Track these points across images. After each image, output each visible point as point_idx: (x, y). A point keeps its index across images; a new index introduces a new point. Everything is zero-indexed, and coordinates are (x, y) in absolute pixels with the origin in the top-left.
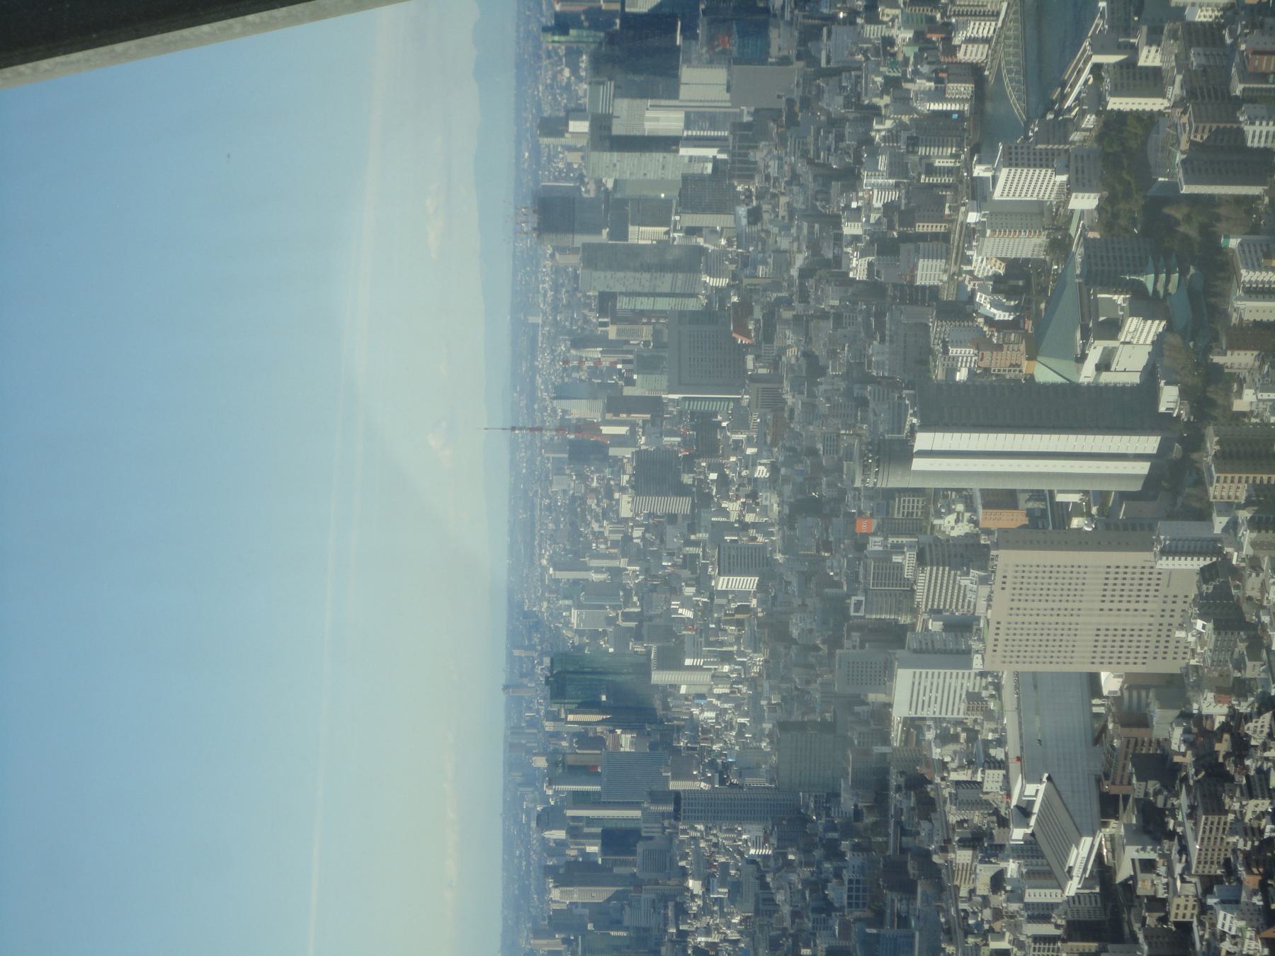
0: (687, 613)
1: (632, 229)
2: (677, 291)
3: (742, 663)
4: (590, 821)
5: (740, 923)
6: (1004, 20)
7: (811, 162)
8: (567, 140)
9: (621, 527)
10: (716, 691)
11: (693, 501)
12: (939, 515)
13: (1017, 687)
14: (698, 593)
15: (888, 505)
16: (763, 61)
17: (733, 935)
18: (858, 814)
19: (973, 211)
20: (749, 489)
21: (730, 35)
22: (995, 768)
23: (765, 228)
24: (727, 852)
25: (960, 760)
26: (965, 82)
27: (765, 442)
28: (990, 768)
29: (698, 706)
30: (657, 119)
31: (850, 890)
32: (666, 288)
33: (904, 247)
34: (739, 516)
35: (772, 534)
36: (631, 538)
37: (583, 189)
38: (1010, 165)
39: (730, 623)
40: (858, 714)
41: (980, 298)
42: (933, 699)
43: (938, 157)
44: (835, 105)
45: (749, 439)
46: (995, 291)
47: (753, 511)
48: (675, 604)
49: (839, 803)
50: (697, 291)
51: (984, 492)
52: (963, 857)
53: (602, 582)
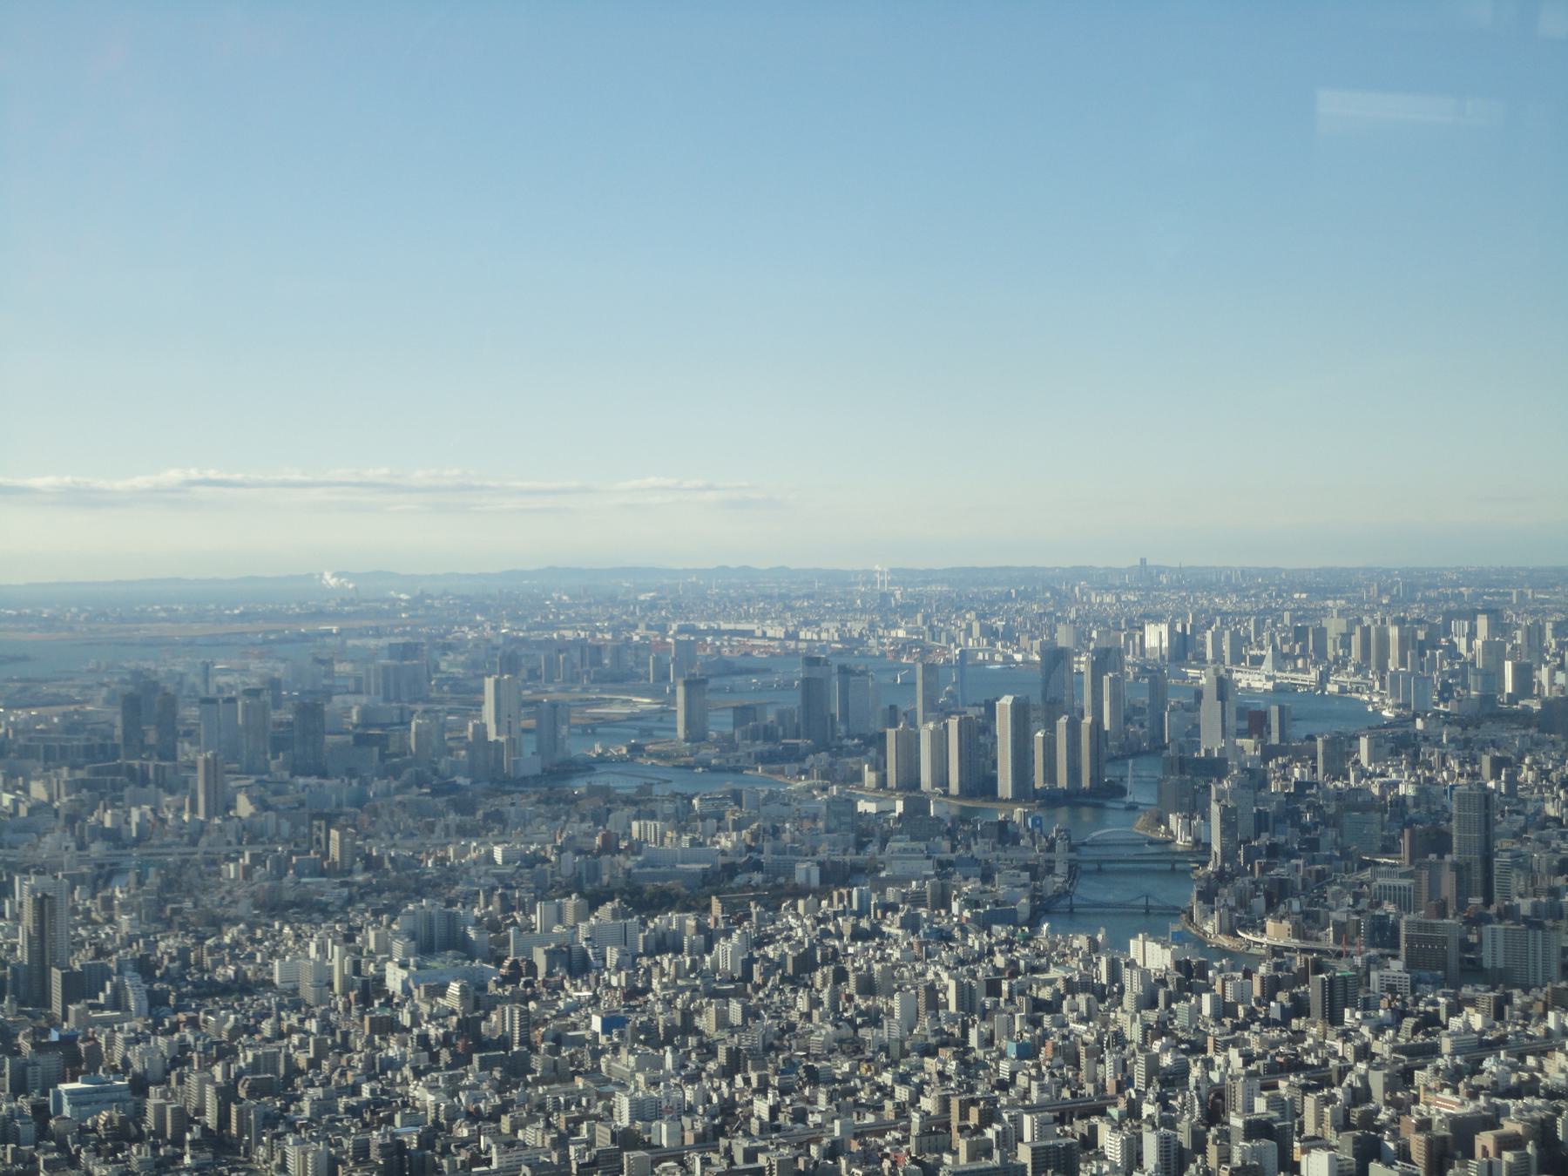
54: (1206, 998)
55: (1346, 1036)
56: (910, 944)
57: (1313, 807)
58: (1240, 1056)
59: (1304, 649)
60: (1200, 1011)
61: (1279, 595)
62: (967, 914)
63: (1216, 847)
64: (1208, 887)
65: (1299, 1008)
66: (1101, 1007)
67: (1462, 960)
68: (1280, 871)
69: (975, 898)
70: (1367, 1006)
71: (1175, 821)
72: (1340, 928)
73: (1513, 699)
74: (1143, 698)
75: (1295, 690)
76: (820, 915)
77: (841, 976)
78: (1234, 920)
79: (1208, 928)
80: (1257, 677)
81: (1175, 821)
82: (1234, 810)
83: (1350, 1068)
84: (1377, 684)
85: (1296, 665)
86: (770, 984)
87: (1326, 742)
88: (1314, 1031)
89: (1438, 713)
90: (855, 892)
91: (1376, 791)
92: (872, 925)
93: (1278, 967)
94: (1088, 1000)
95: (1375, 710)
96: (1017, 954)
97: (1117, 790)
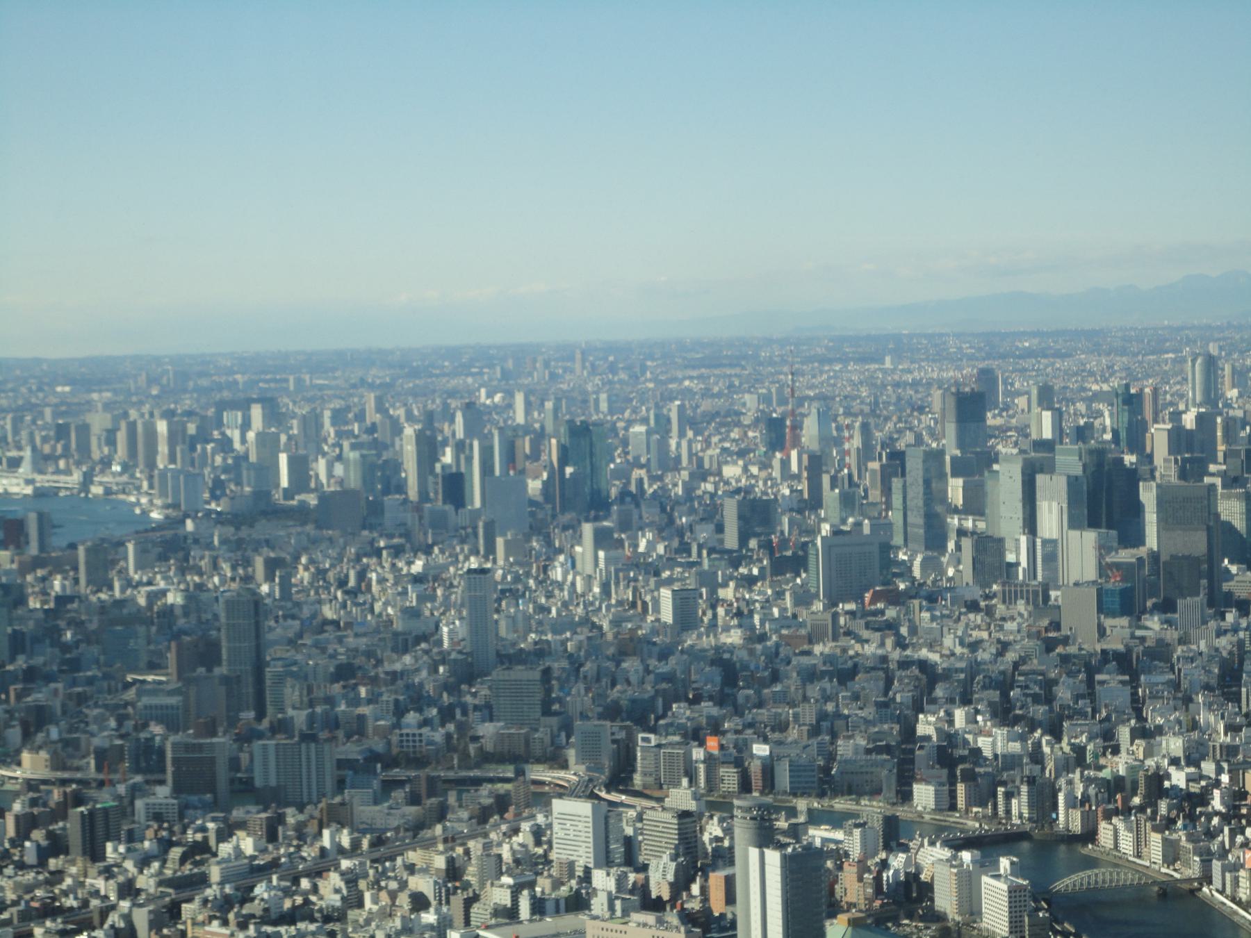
0: (642, 549)
1: (959, 482)
2: (909, 529)
3: (600, 608)
4: (469, 459)
5: (388, 615)
6: (1134, 863)
7: (1016, 665)
8: (1036, 410)
9: (715, 466)
10: (578, 579)
11: (735, 551)
12: (721, 820)
13: (576, 932)
14: (660, 557)
15: (730, 763)
16: (1100, 610)
17: (378, 607)
18: (475, 739)
19: (972, 856)
20: (746, 612)
21: (1121, 581)
22: (512, 897)
23: (962, 617)
24: (446, 598)
25: (520, 852)
26: (1082, 826)
27: (782, 627)
28: (512, 892)
29: (566, 560)
30: (1050, 511)
31: (414, 735)
32: (910, 520)
33: (945, 772)
34: (723, 600)
35: (708, 636)
36: (705, 480)
37: (996, 412)
38: (1010, 892)
39: (635, 590)
40: (559, 736)
41: (902, 857)
42: (568, 832)
43: (1019, 802)
44: (1063, 693)
45: (785, 609)
46: (907, 874)
47: (727, 614)
48: (649, 535)
49: (483, 721)
50: (909, 545)
51: (734, 875)
52: (440, 862)
53: (668, 446)
55: (108, 873)
57: (77, 624)
59: (66, 448)
61: (40, 389)
65: (57, 846)
67: (232, 781)
68: (39, 696)
70: (131, 838)
72: (101, 755)
73: (288, 494)
75: (56, 494)
80: (15, 481)
83: (113, 907)
84: (145, 485)
87: (88, 551)
88: (73, 870)
89: (209, 512)
91: (142, 601)
93: (34, 803)
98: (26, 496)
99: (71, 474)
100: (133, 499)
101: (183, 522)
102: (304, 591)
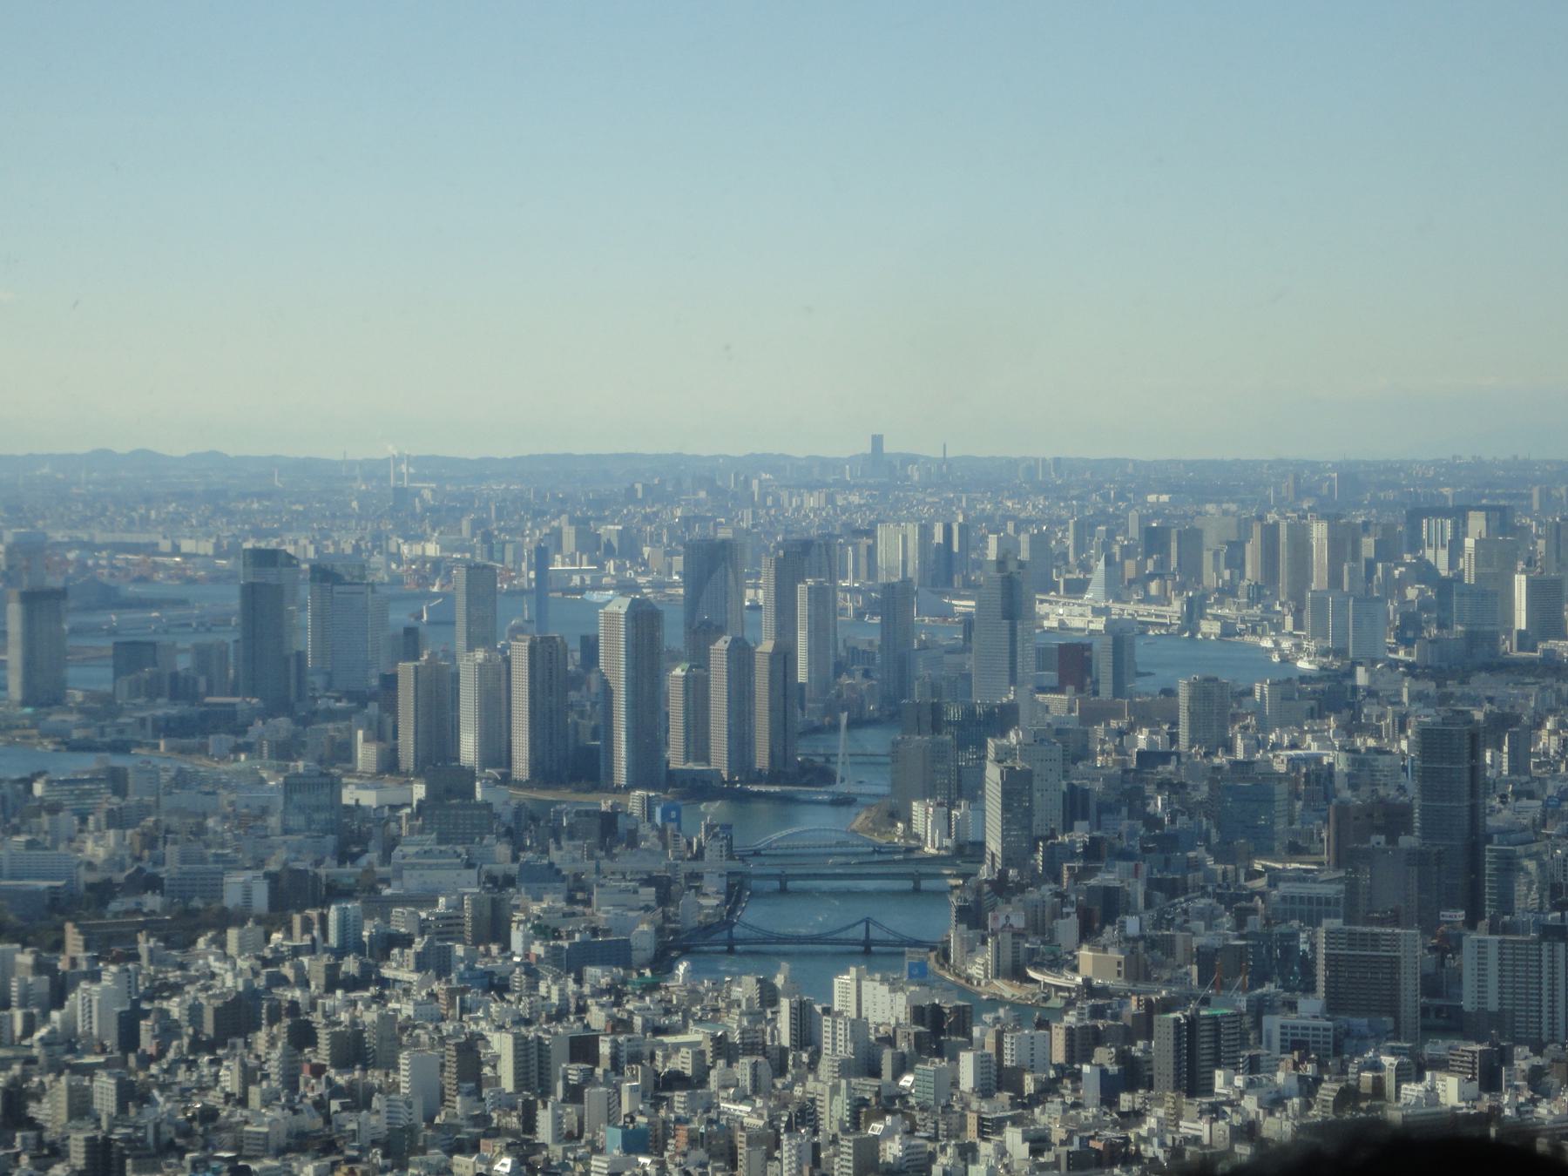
54: (967, 1060)
55: (1215, 1112)
56: (433, 996)
57: (1174, 788)
58: (1025, 1140)
59: (1162, 564)
60: (955, 1083)
62: (538, 949)
63: (994, 845)
64: (978, 903)
65: (1133, 1075)
66: (779, 1083)
67: (1425, 1011)
68: (1107, 878)
69: (553, 925)
70: (1254, 1066)
71: (922, 814)
73: (1524, 640)
74: (869, 633)
75: (1143, 633)
76: (267, 953)
77: (303, 1036)
78: (1022, 956)
79: (976, 971)
80: (1077, 610)
81: (922, 814)
82: (1027, 776)
84: (1289, 621)
85: (1147, 592)
86: (171, 1055)
88: (1161, 1112)
89: (1393, 665)
90: (333, 914)
91: (1280, 767)
92: (363, 965)
93: (1097, 1012)
94: (755, 1066)
95: (1285, 660)
96: (629, 1007)
97: (822, 775)
98: (1092, 632)
99: (1169, 604)
100: (1267, 643)
101: (1351, 674)
102: (1547, 762)
